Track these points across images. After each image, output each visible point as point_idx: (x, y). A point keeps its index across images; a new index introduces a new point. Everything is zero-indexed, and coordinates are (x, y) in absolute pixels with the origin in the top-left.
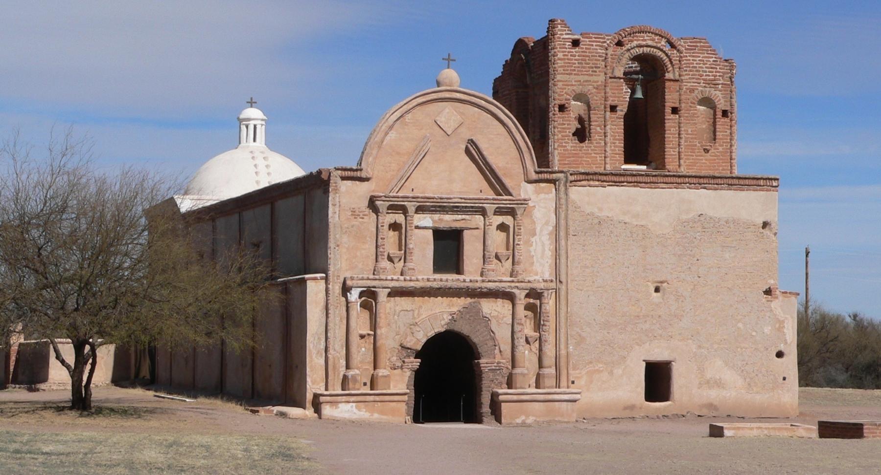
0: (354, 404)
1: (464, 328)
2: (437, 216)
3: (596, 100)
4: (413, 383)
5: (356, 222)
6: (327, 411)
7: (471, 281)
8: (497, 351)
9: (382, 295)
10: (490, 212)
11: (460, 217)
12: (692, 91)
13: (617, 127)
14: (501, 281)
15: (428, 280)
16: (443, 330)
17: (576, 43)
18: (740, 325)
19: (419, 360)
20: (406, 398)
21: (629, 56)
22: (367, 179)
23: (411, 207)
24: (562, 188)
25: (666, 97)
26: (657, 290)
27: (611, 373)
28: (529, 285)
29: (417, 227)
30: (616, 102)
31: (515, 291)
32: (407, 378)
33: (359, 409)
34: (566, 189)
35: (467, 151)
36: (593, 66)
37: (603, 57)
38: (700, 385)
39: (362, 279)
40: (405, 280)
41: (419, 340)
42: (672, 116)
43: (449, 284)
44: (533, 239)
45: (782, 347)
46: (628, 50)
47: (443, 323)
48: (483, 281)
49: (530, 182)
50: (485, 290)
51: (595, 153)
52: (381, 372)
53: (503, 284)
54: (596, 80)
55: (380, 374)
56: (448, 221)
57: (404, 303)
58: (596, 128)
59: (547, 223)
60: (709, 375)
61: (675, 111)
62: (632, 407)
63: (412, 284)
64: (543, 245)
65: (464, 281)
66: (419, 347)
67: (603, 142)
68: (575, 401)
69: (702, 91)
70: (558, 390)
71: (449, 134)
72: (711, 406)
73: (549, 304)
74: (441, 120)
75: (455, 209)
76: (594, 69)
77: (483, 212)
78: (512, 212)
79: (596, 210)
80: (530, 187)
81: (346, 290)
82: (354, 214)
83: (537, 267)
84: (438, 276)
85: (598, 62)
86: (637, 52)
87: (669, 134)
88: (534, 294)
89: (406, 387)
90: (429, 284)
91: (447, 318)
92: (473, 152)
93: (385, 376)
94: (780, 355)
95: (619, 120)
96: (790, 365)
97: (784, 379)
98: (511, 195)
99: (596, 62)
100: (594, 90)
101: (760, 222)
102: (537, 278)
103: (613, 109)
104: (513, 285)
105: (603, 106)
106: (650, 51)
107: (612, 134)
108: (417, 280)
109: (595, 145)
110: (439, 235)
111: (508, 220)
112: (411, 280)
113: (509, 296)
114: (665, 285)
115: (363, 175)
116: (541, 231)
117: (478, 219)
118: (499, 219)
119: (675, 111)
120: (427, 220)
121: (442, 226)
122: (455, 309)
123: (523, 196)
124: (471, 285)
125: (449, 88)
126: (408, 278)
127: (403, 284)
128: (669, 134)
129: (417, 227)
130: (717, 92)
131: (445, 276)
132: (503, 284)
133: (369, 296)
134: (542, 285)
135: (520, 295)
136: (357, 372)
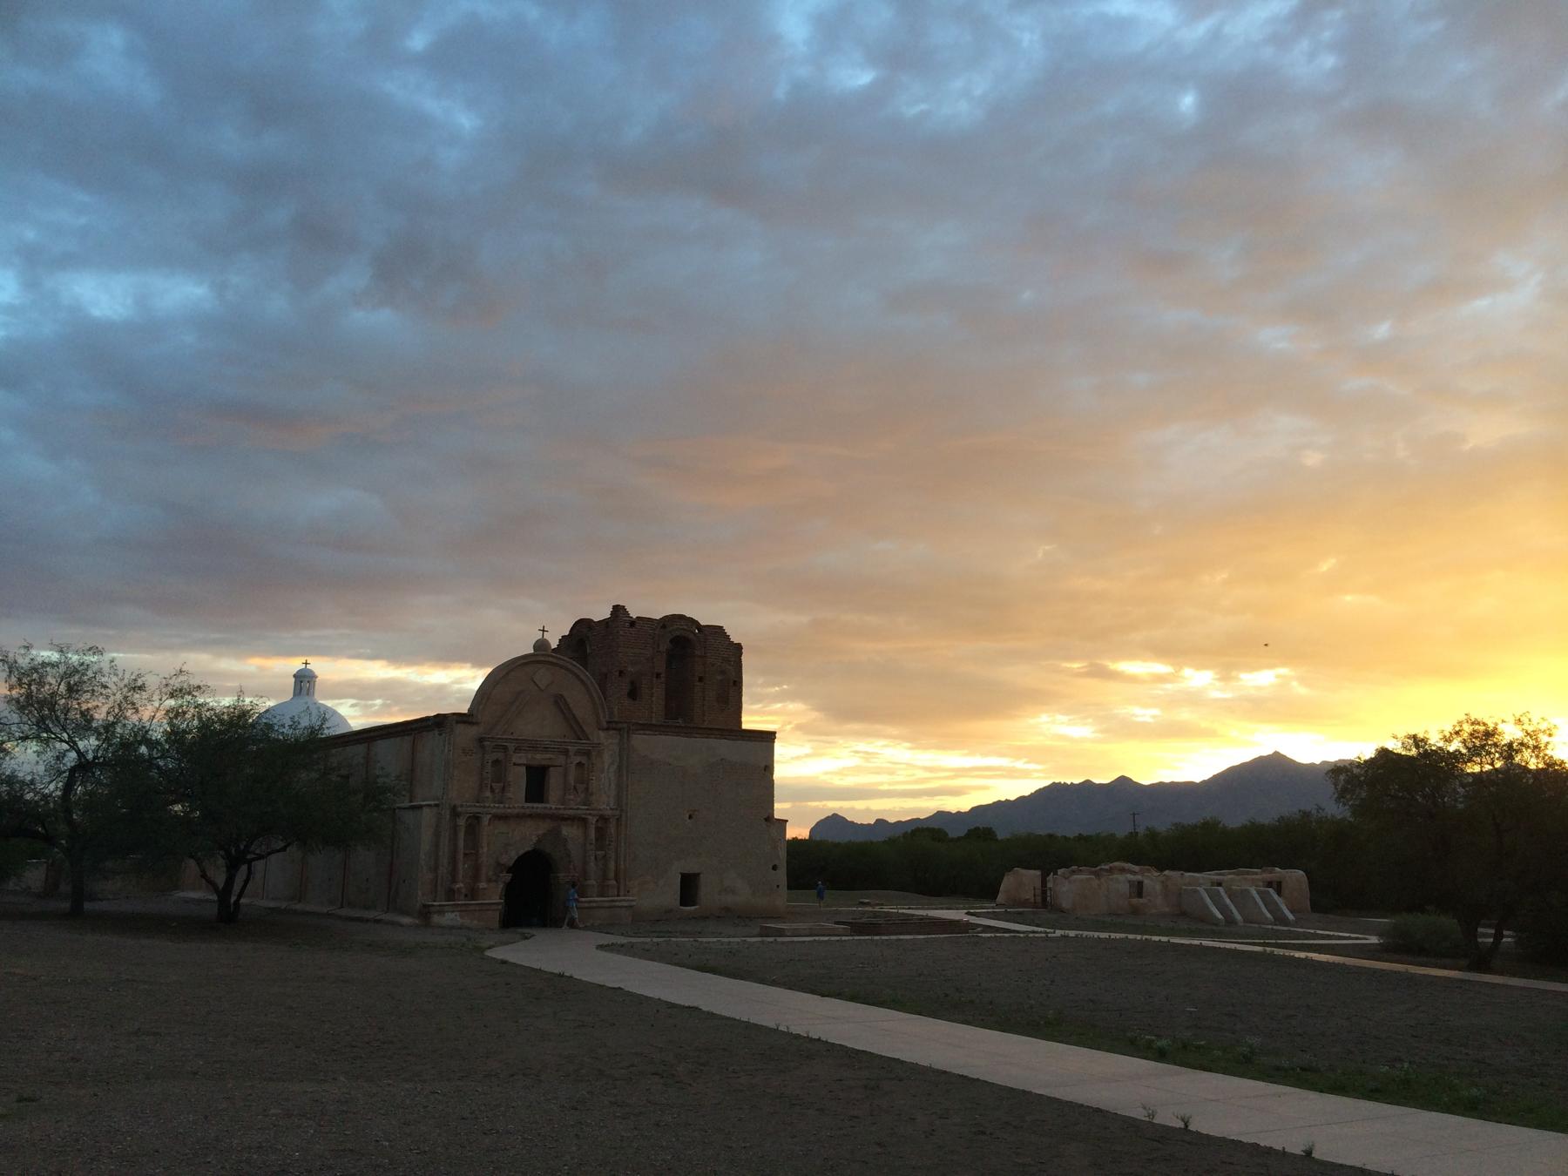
0: (458, 914)
4: (504, 893)
6: (436, 919)
7: (556, 809)
8: (571, 867)
9: (486, 820)
11: (548, 756)
14: (578, 809)
15: (523, 807)
16: (530, 849)
17: (633, 623)
19: (511, 875)
20: (500, 907)
22: (477, 724)
23: (511, 746)
24: (625, 735)
26: (690, 817)
28: (601, 813)
29: (515, 764)
31: (590, 817)
32: (500, 890)
33: (461, 917)
34: (628, 737)
35: (556, 702)
39: (470, 806)
40: (504, 807)
41: (511, 857)
42: (698, 684)
43: (539, 811)
44: (602, 776)
45: (776, 862)
46: (670, 632)
47: (531, 843)
48: (565, 809)
49: (603, 730)
50: (566, 816)
52: (483, 885)
53: (579, 812)
55: (481, 887)
56: (539, 758)
59: (612, 763)
61: (701, 679)
62: (671, 911)
63: (509, 811)
64: (609, 779)
65: (551, 808)
66: (511, 865)
68: (631, 907)
69: (720, 666)
70: (619, 898)
71: (543, 688)
72: (727, 909)
73: (612, 829)
75: (546, 750)
78: (587, 754)
80: (602, 734)
88: (603, 819)
89: (498, 897)
90: (523, 811)
91: (534, 839)
92: (560, 703)
93: (485, 889)
94: (775, 868)
96: (781, 876)
97: (778, 886)
98: (588, 739)
101: (763, 765)
102: (605, 806)
103: (658, 676)
104: (588, 812)
108: (514, 807)
110: (530, 769)
111: (584, 760)
112: (509, 808)
114: (696, 813)
115: (474, 721)
116: (608, 769)
117: (561, 760)
118: (578, 759)
119: (701, 679)
120: (520, 758)
121: (535, 763)
122: (540, 832)
123: (596, 741)
124: (555, 812)
125: (544, 653)
126: (507, 806)
127: (503, 811)
129: (515, 764)
130: (731, 668)
131: (535, 805)
132: (579, 812)
134: (609, 812)
135: (592, 820)
136: (462, 885)
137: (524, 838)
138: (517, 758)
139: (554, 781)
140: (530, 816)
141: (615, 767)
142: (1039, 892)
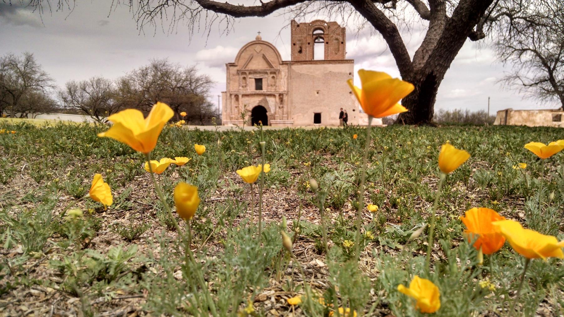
1: (263, 105)
2: (255, 75)
3: (304, 41)
5: (234, 77)
9: (240, 96)
10: (269, 74)
12: (332, 37)
17: (298, 26)
18: (342, 102)
23: (247, 73)
26: (318, 93)
27: (304, 116)
31: (276, 94)
38: (329, 119)
41: (251, 108)
49: (280, 64)
56: (258, 76)
57: (246, 99)
58: (304, 49)
59: (285, 76)
60: (332, 116)
73: (285, 98)
74: (256, 49)
75: (260, 73)
77: (267, 73)
79: (299, 72)
80: (281, 66)
81: (231, 95)
82: (234, 75)
83: (283, 88)
84: (256, 91)
91: (258, 102)
92: (264, 57)
94: (354, 110)
101: (348, 72)
111: (275, 75)
113: (274, 96)
115: (235, 65)
133: (237, 97)
137: (254, 102)
138: (250, 76)
139: (264, 84)
140: (255, 94)
141: (286, 77)
142: (503, 120)
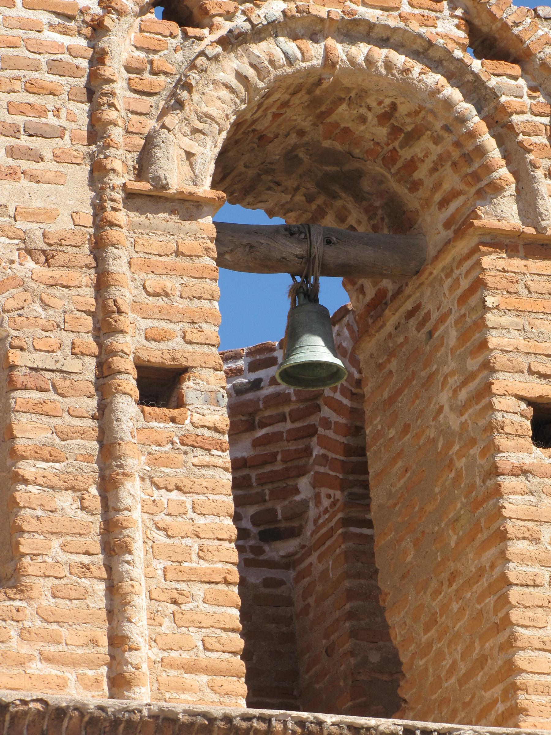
13: (188, 500)
21: (241, 78)
25: (494, 340)
30: (177, 343)
36: (20, 120)
37: (73, 73)
51: (47, 659)
54: (37, 204)
67: (101, 587)
76: (25, 141)
85: (50, 102)
86: (290, 61)
87: (523, 559)
95: (203, 457)
99: (32, 99)
100: (30, 264)
105: (91, 363)
106: (369, 60)
107: (160, 537)
109: (47, 602)
128: (523, 559)
